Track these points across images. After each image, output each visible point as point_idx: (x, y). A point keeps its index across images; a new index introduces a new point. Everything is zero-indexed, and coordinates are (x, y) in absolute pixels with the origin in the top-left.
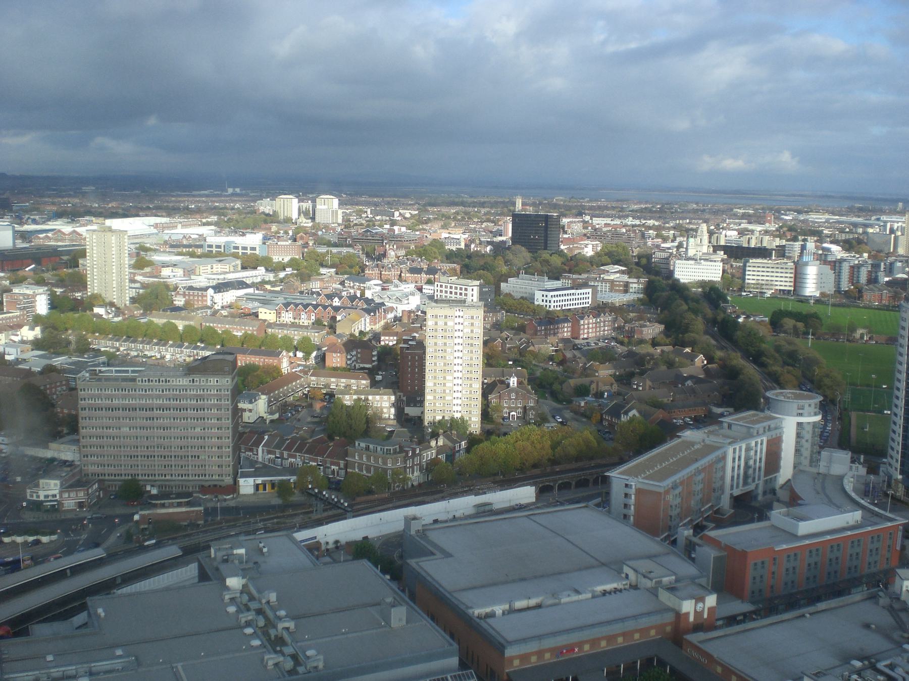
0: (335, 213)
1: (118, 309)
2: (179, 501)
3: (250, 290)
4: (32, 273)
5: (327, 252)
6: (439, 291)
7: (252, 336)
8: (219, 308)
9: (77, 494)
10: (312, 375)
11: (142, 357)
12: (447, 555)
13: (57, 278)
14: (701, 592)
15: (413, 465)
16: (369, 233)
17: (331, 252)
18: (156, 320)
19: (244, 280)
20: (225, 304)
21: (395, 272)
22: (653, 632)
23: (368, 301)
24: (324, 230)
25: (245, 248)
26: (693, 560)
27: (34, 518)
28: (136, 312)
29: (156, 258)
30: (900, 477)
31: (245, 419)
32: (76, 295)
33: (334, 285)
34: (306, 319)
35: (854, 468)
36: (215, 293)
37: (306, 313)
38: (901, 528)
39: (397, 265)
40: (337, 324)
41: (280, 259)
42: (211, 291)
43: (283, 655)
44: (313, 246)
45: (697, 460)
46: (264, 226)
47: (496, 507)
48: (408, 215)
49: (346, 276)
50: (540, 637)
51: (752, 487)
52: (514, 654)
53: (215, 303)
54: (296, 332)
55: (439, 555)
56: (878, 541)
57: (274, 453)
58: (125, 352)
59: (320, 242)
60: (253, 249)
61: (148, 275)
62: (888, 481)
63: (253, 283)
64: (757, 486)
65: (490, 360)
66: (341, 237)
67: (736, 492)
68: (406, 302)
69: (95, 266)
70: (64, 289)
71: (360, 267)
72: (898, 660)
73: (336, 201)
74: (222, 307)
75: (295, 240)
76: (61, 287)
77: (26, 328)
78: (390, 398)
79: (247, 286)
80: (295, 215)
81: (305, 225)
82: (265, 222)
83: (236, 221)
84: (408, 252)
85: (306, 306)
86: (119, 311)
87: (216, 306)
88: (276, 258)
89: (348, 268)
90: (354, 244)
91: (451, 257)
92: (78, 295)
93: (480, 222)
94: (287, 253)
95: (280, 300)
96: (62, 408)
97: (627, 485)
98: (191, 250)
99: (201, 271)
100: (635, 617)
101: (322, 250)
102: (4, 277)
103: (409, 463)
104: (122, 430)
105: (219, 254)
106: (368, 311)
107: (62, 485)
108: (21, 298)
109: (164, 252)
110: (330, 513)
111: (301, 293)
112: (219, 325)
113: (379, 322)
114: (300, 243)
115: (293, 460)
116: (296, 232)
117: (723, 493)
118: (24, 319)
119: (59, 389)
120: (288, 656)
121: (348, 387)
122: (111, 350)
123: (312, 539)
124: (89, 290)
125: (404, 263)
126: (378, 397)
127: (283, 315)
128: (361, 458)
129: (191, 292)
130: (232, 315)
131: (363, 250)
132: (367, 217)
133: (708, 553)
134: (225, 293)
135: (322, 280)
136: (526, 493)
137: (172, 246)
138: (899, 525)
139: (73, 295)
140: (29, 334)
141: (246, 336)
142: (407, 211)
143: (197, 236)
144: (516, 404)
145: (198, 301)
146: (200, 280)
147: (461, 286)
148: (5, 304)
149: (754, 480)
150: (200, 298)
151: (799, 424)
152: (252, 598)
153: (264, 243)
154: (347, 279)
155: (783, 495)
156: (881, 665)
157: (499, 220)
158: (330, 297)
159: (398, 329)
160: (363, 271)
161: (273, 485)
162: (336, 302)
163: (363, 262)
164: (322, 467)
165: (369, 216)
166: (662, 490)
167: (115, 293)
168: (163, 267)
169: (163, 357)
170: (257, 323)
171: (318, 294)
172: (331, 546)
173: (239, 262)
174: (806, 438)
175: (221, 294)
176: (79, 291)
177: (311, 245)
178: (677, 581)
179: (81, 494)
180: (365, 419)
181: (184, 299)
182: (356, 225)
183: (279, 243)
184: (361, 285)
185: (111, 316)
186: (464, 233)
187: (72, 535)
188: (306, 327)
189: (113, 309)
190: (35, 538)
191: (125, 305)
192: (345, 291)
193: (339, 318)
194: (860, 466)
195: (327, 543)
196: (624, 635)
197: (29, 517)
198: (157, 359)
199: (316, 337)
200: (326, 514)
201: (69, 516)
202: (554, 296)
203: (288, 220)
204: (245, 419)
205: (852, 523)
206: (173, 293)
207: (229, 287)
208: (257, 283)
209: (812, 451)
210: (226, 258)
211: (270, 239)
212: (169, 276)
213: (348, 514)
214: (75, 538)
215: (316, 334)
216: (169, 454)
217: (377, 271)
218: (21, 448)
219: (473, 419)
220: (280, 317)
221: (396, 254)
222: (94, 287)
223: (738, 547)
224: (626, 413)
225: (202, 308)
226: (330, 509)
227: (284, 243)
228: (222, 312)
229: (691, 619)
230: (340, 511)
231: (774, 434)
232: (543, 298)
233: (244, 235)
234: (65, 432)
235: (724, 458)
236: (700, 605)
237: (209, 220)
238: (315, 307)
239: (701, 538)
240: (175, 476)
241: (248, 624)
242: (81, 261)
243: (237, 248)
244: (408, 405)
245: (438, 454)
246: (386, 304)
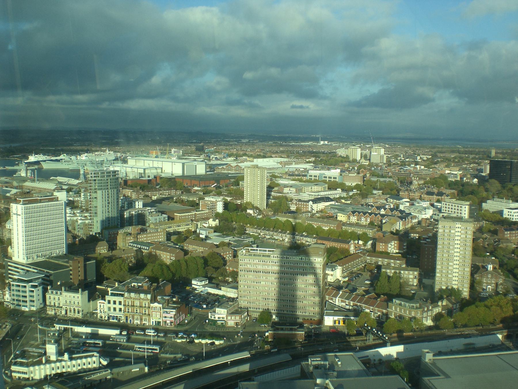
0: (382, 157)
1: (260, 210)
2: (291, 327)
3: (333, 203)
4: (215, 189)
5: (378, 180)
6: (444, 207)
7: (334, 230)
8: (315, 212)
9: (235, 318)
10: (367, 256)
11: (272, 239)
13: (229, 192)
15: (428, 316)
16: (402, 170)
17: (380, 180)
18: (280, 218)
19: (329, 196)
20: (318, 210)
21: (417, 194)
23: (402, 212)
24: (375, 167)
25: (330, 178)
27: (212, 329)
28: (269, 213)
29: (281, 182)
31: (329, 280)
32: (238, 202)
33: (381, 201)
34: (365, 221)
36: (313, 204)
37: (365, 217)
39: (419, 190)
40: (383, 225)
41: (350, 184)
42: (311, 203)
44: (369, 177)
46: (341, 164)
48: (425, 159)
49: (388, 196)
53: (313, 210)
54: (359, 229)
57: (345, 302)
58: (263, 236)
59: (373, 174)
60: (335, 178)
61: (276, 191)
63: (334, 198)
65: (476, 251)
66: (386, 171)
68: (424, 213)
69: (249, 187)
70: (232, 198)
71: (397, 190)
73: (382, 151)
74: (317, 212)
75: (358, 173)
76: (230, 197)
77: (211, 220)
78: (414, 273)
79: (332, 200)
80: (358, 158)
81: (364, 164)
82: (342, 162)
83: (325, 160)
84: (426, 182)
85: (365, 213)
86: (260, 212)
87: (313, 211)
88: (348, 184)
89: (389, 190)
90: (393, 176)
91: (451, 185)
92: (239, 202)
93: (469, 163)
94: (354, 181)
95: (350, 209)
96: (229, 267)
98: (300, 177)
99: (306, 190)
101: (374, 179)
102: (200, 190)
104: (261, 283)
105: (315, 181)
106: (401, 218)
107: (227, 312)
108: (209, 203)
109: (285, 178)
111: (362, 205)
112: (315, 223)
113: (408, 224)
114: (361, 175)
116: (359, 169)
118: (210, 215)
119: (228, 256)
121: (389, 264)
122: (256, 234)
124: (245, 199)
125: (423, 188)
126: (407, 272)
127: (351, 218)
128: (396, 309)
129: (300, 203)
130: (323, 217)
131: (398, 180)
132: (401, 159)
134: (319, 204)
135: (374, 198)
137: (290, 175)
139: (236, 202)
140: (213, 223)
141: (330, 230)
142: (425, 156)
143: (303, 169)
144: (492, 281)
145: (304, 208)
146: (305, 196)
147: (458, 205)
148: (200, 206)
150: (305, 206)
153: (341, 175)
154: (389, 197)
157: (481, 162)
158: (379, 208)
159: (419, 229)
160: (398, 193)
162: (383, 212)
163: (398, 187)
164: (372, 313)
165: (402, 159)
167: (258, 202)
168: (285, 187)
169: (283, 240)
170: (337, 223)
171: (372, 206)
172: (377, 362)
173: (327, 186)
175: (316, 204)
176: (239, 199)
177: (368, 176)
179: (238, 318)
180: (399, 286)
181: (296, 207)
182: (394, 164)
183: (350, 175)
184: (397, 201)
185: (256, 215)
186: (459, 170)
187: (232, 341)
188: (365, 226)
189: (258, 211)
190: (212, 341)
191: (264, 209)
192: (388, 205)
193: (384, 221)
195: (375, 360)
197: (209, 329)
198: (280, 241)
199: (370, 233)
201: (231, 330)
202: (516, 212)
203: (355, 161)
204: (329, 280)
206: (290, 203)
207: (321, 200)
208: (337, 198)
210: (319, 183)
211: (344, 172)
212: (288, 193)
214: (233, 343)
215: (371, 231)
216: (287, 299)
217: (406, 193)
218: (206, 288)
219: (465, 289)
220: (349, 219)
221: (418, 183)
222: (247, 198)
225: (306, 212)
227: (353, 175)
228: (317, 215)
232: (509, 213)
233: (329, 169)
234: (230, 281)
237: (310, 160)
238: (370, 214)
240: (289, 312)
242: (241, 183)
243: (326, 177)
245: (442, 310)
246: (412, 213)
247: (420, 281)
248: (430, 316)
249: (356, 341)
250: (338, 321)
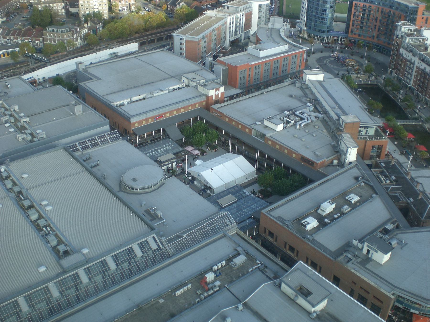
12: (99, 79)
14: (217, 86)
15: (77, 37)
22: (197, 106)
26: (213, 72)
30: (305, 28)
35: (285, 25)
38: (306, 51)
43: (26, 134)
45: (213, 25)
47: (120, 54)
50: (146, 112)
51: (239, 36)
52: (135, 121)
55: (95, 79)
56: (296, 58)
57: (6, 38)
62: (300, 30)
64: (241, 35)
67: (232, 39)
72: (304, 110)
78: (61, 4)
97: (181, 39)
100: (188, 99)
103: (75, 36)
110: (39, 64)
115: (16, 40)
117: (226, 40)
120: (28, 134)
123: (31, 78)
126: (55, 5)
128: (50, 36)
133: (220, 68)
136: (133, 46)
138: (305, 50)
149: (239, 33)
151: (260, 6)
152: (6, 110)
155: (253, 39)
156: (297, 113)
161: (8, 54)
164: (31, 42)
166: (198, 40)
172: (41, 80)
174: (263, 12)
178: (206, 82)
180: (50, 16)
194: (288, 24)
195: (39, 79)
196: (184, 108)
200: (36, 65)
205: (284, 50)
209: (266, 18)
213: (48, 64)
219: (104, 12)
223: (233, 65)
224: (179, 4)
226: (38, 62)
229: (214, 98)
230: (43, 63)
231: (248, 10)
235: (226, 23)
236: (217, 92)
239: (216, 61)
241: (6, 122)
244: (71, 7)
245: (89, 30)
247: (67, 11)
248: (79, 37)
249: (21, 67)
250: (2, 54)
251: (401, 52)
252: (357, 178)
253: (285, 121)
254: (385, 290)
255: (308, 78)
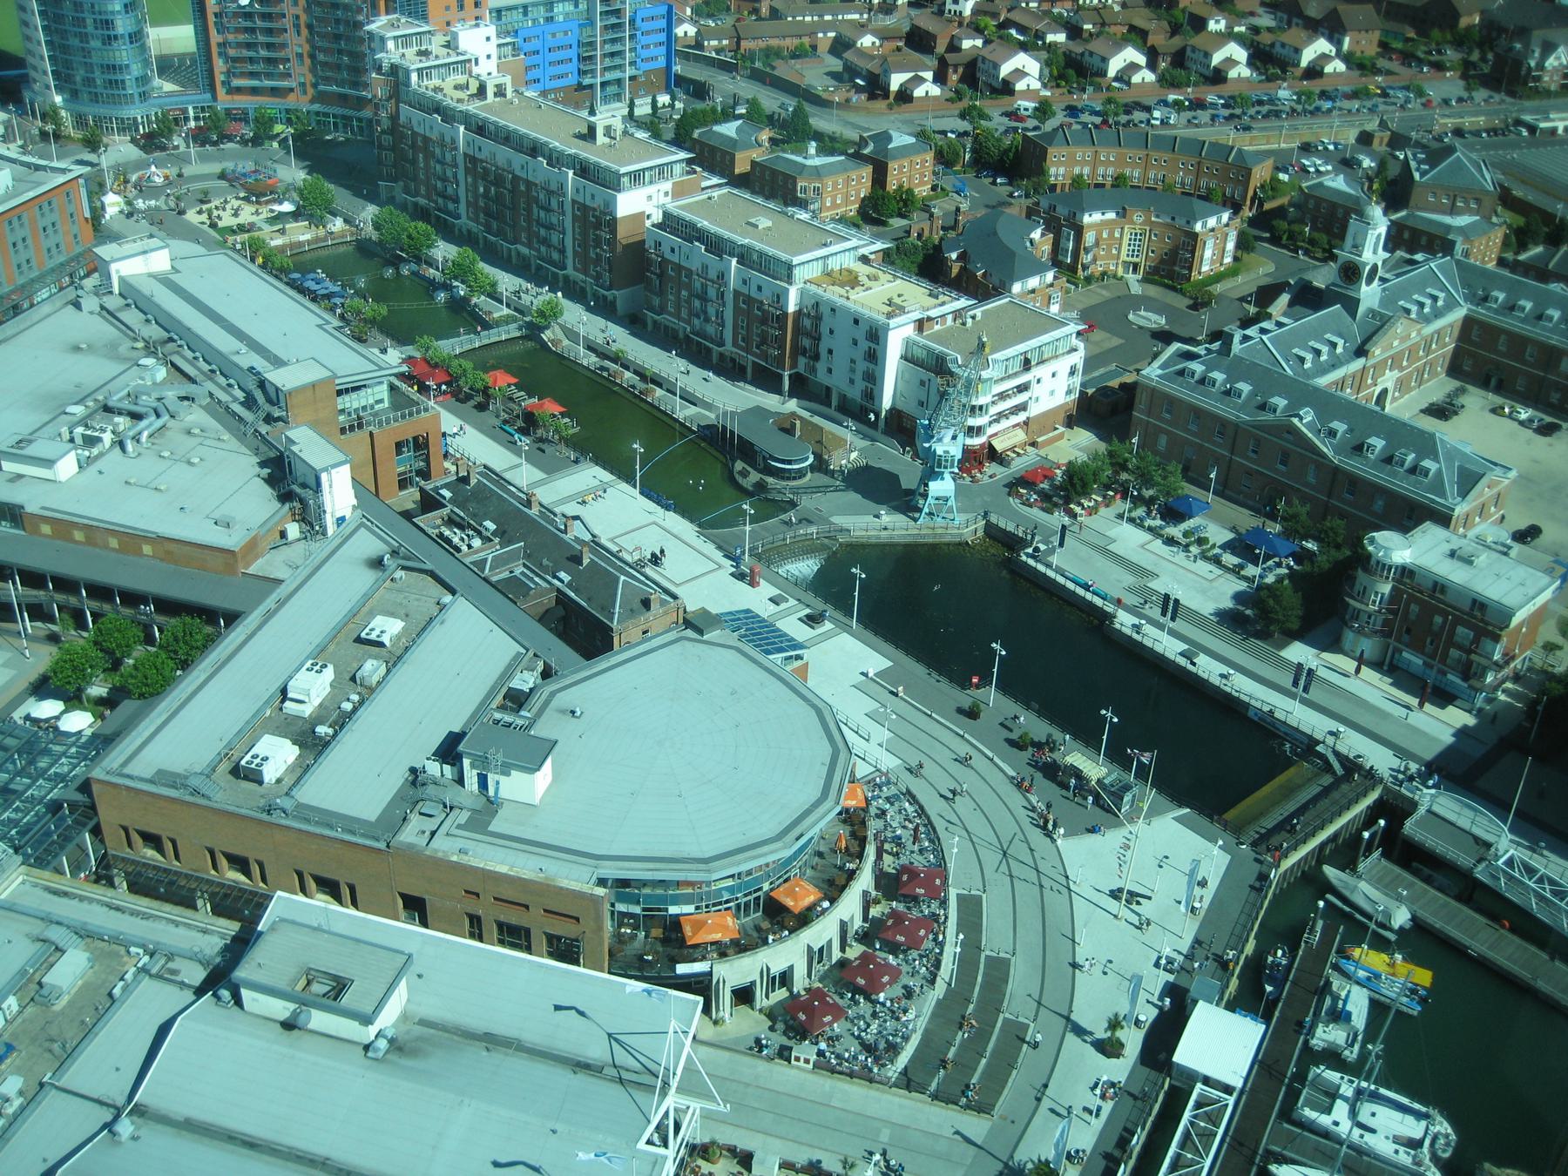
251: (402, 119)
252: (377, 563)
253: (79, 440)
254: (576, 879)
255: (118, 271)
